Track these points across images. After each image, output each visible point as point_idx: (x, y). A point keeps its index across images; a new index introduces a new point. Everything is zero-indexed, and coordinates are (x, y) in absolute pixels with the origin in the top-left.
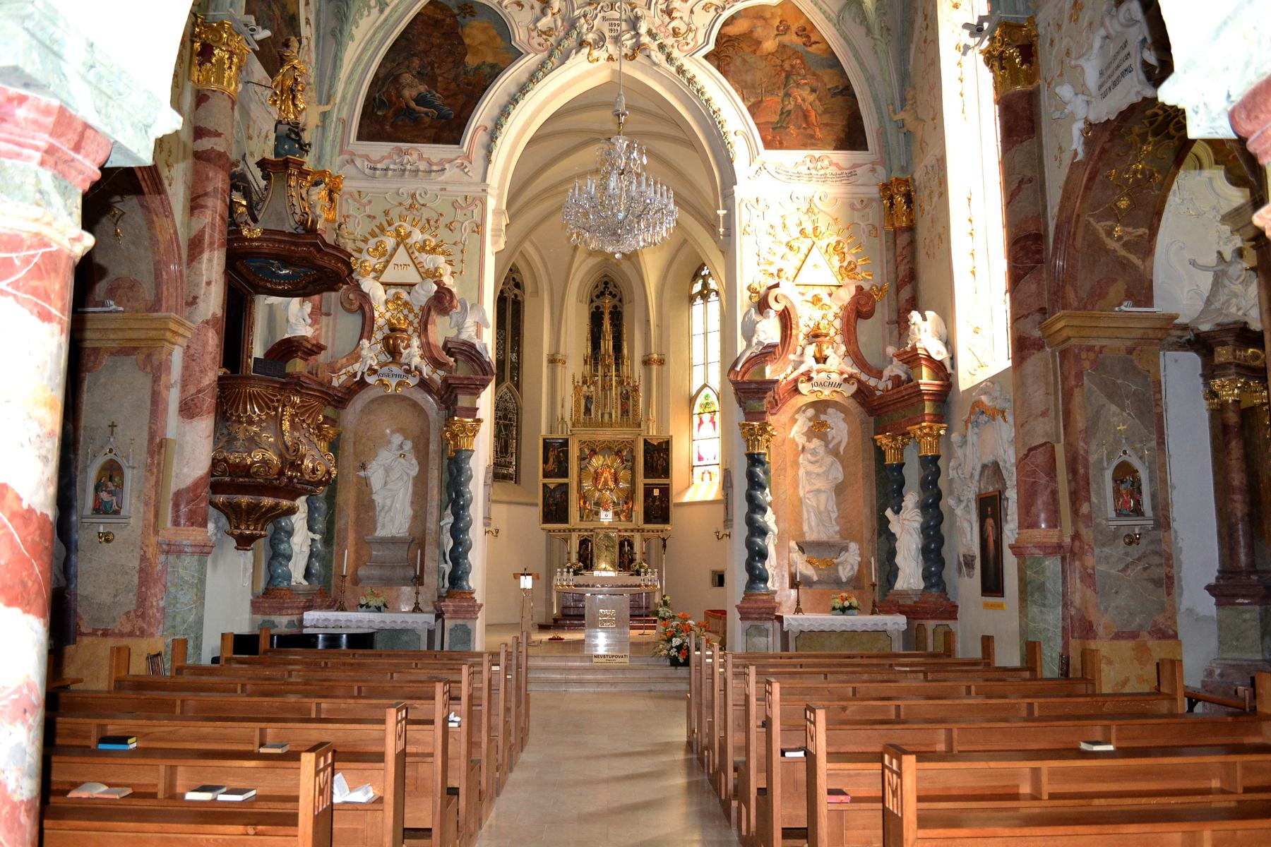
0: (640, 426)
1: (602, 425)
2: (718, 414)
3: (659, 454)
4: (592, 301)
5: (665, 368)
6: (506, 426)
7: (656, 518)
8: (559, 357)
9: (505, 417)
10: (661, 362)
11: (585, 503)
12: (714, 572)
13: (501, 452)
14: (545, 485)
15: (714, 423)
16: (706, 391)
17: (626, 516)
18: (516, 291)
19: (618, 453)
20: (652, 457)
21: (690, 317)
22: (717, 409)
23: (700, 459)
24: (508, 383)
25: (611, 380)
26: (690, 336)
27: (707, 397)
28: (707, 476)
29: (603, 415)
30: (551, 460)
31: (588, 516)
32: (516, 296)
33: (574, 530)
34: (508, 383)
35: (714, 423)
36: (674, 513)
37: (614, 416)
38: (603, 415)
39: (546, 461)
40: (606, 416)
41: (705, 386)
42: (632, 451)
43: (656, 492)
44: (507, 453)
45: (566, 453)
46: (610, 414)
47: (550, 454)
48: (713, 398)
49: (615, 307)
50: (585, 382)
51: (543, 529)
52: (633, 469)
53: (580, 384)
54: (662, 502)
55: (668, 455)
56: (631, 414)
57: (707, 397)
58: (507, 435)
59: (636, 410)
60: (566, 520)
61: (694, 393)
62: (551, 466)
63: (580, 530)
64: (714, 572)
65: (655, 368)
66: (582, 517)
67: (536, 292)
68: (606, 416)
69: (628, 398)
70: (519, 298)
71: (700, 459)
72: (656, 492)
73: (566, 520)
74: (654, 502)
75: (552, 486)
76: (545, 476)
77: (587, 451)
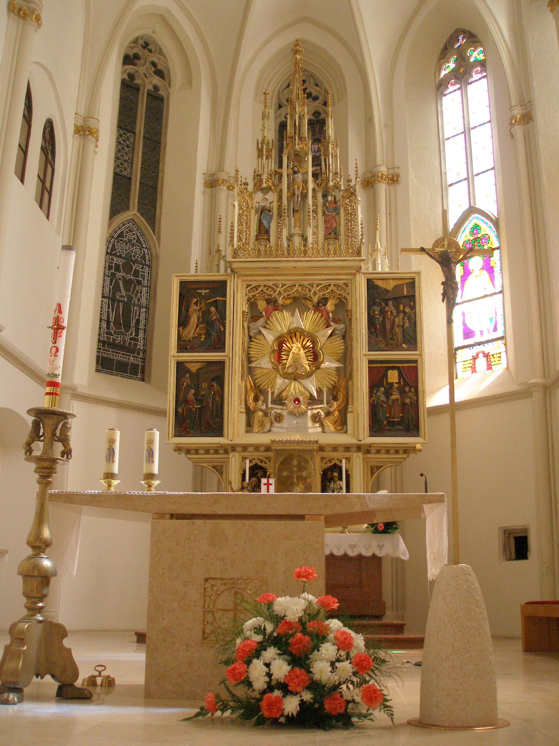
0: (359, 253)
1: (290, 252)
2: (496, 253)
3: (397, 308)
4: (280, 107)
5: (400, 188)
6: (128, 284)
7: (392, 424)
8: (223, 176)
9: (127, 268)
10: (394, 180)
11: (256, 399)
12: (507, 533)
13: (117, 323)
14: (180, 365)
15: (490, 270)
16: (475, 219)
17: (335, 423)
18: (156, 80)
19: (320, 305)
20: (383, 313)
21: (438, 114)
22: (496, 244)
23: (468, 333)
24: (133, 213)
25: (305, 182)
26: (440, 142)
27: (476, 229)
28: (481, 362)
29: (290, 238)
30: (194, 319)
31: (262, 424)
32: (156, 88)
33: (234, 448)
34: (133, 213)
35: (490, 270)
36: (425, 421)
37: (310, 240)
38: (290, 238)
39: (183, 322)
40: (297, 240)
41: (472, 210)
42: (342, 304)
43: (393, 376)
44: (127, 327)
45: (221, 308)
46: (305, 239)
47: (193, 307)
48: (487, 229)
49: (317, 114)
50: (258, 186)
51: (178, 449)
52: (346, 337)
53: (250, 188)
54: (402, 392)
55: (413, 308)
56: (342, 238)
57: (476, 229)
58: (130, 298)
59: (350, 230)
60: (218, 431)
61: (451, 226)
62: (191, 331)
63: (245, 448)
64: (507, 533)
65: (382, 188)
66: (249, 424)
67: (189, 82)
68: (297, 240)
69: (337, 210)
70: (162, 92)
71: (468, 333)
72: (393, 376)
73: (218, 431)
74: (388, 394)
75: (194, 368)
76: (182, 347)
77: (262, 305)
